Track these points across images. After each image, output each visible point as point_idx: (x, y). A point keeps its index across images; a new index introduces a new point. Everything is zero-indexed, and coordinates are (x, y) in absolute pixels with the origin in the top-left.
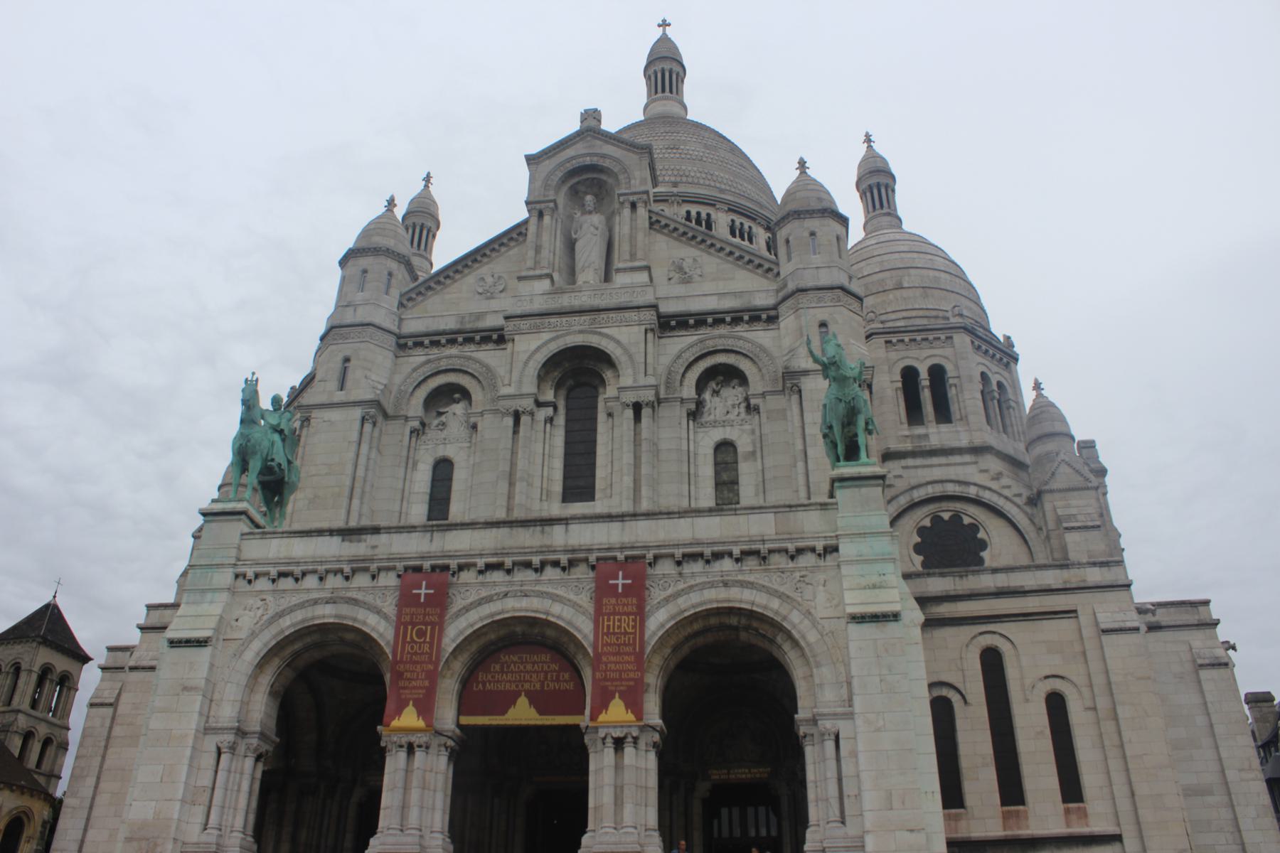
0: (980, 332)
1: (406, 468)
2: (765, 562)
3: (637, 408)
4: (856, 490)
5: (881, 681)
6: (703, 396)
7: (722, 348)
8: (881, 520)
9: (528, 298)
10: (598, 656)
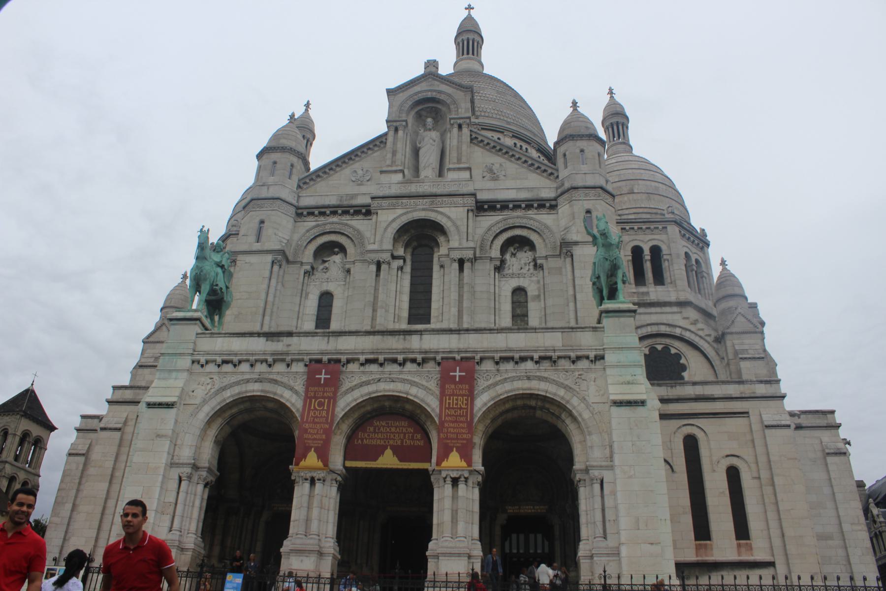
0: (685, 225)
1: (301, 297)
4: (616, 319)
5: (633, 445)
6: (505, 257)
7: (519, 225)
8: (633, 340)
10: (442, 423)
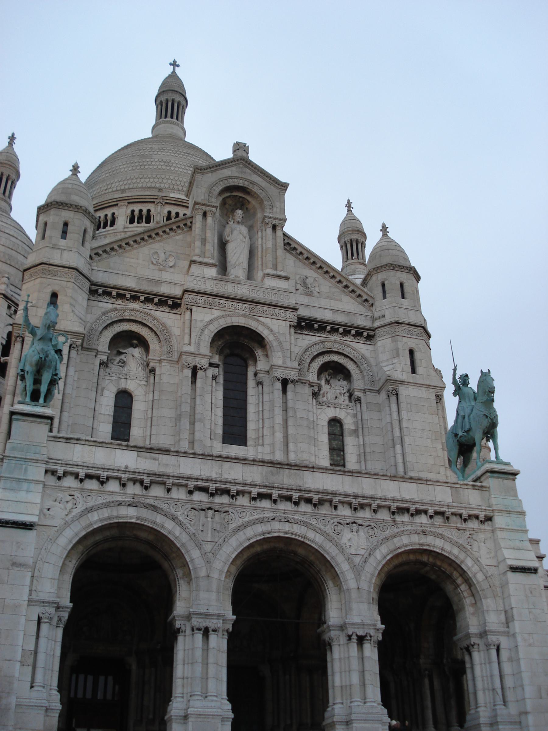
2: (448, 521)
3: (285, 383)
4: (501, 480)
5: (530, 612)
7: (337, 350)
9: (202, 280)
